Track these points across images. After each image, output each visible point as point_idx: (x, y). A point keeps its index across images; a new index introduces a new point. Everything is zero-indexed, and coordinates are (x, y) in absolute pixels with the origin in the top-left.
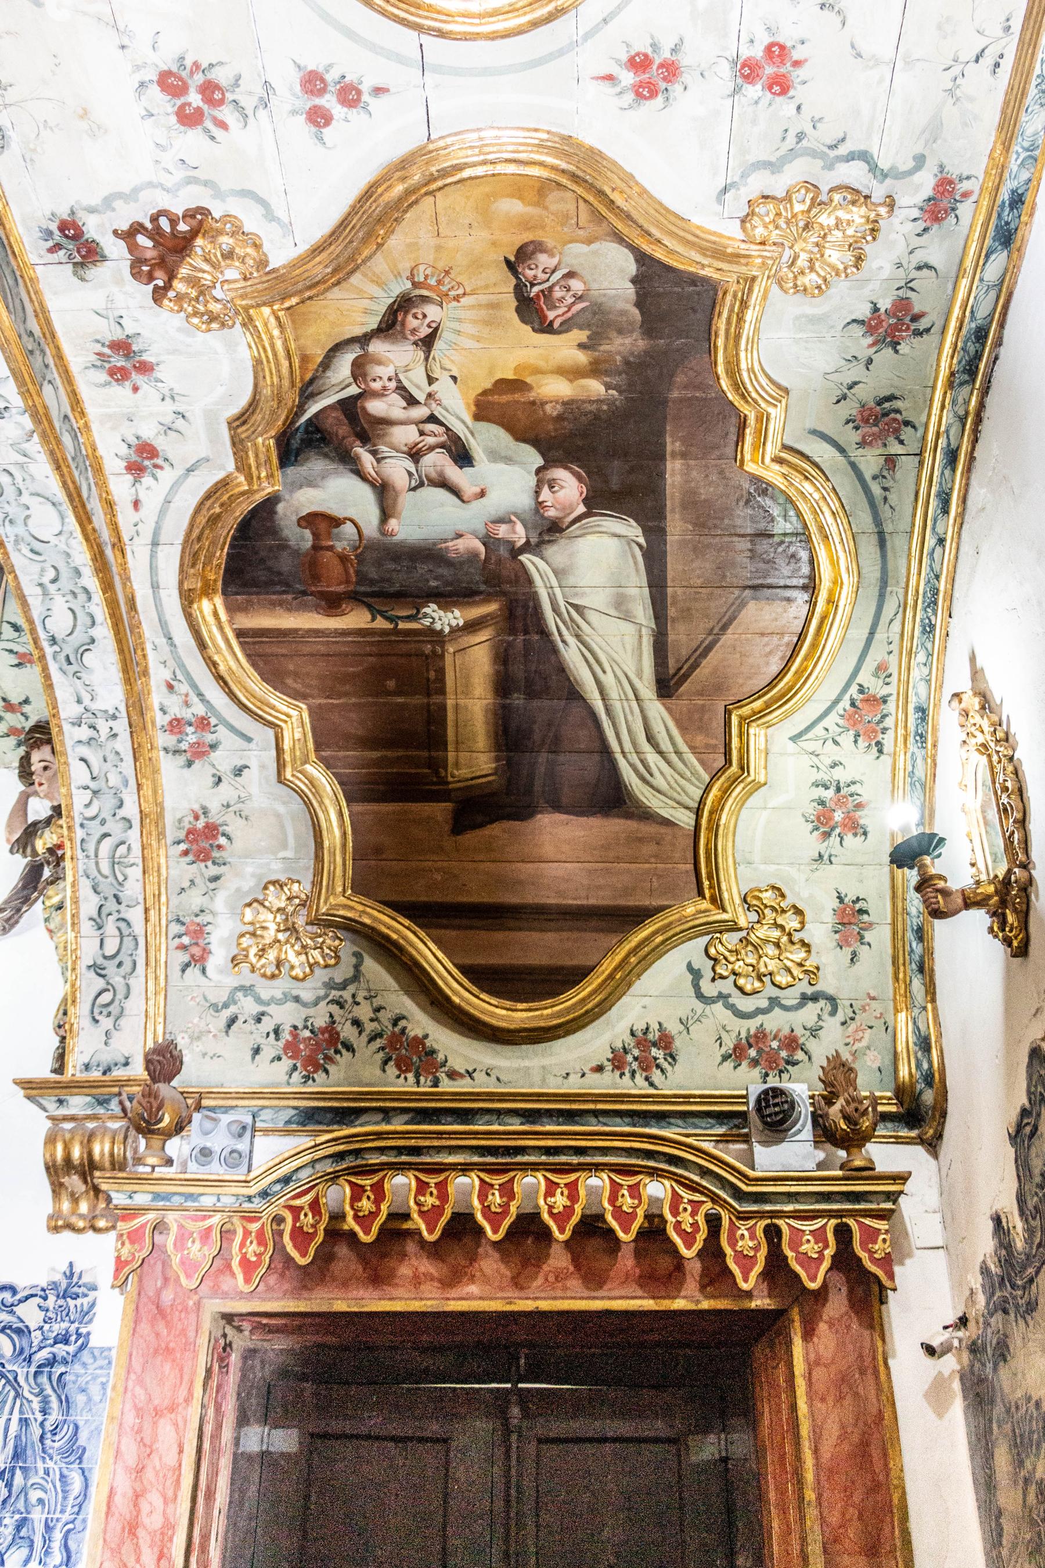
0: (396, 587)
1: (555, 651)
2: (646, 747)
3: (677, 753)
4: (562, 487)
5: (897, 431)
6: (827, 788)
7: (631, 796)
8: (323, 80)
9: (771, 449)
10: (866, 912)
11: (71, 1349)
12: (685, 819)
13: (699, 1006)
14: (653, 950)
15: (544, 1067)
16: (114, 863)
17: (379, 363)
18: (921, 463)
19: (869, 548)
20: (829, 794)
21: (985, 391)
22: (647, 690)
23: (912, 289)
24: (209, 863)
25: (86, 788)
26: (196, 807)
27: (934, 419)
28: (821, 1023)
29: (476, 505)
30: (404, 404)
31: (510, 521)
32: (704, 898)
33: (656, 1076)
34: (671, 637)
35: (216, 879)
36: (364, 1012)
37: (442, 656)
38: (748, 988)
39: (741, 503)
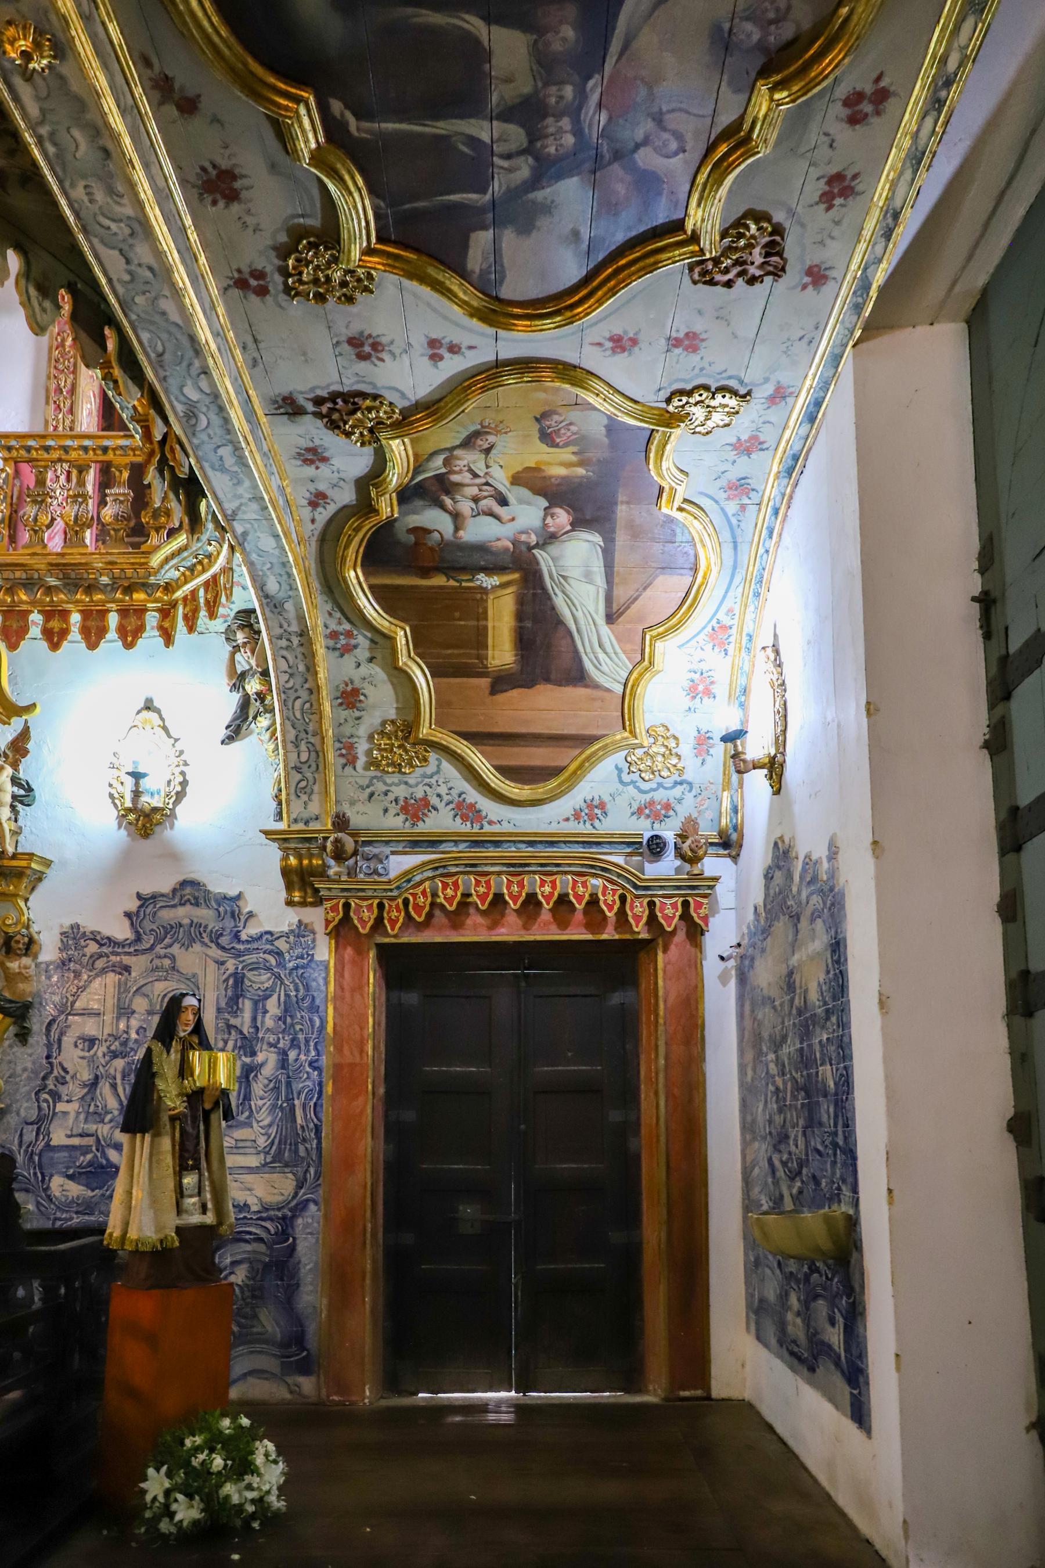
0: (462, 565)
1: (550, 598)
7: (589, 676)
11: (305, 961)
12: (618, 689)
18: (760, 510)
19: (728, 549)
22: (601, 620)
34: (615, 593)
37: (486, 601)
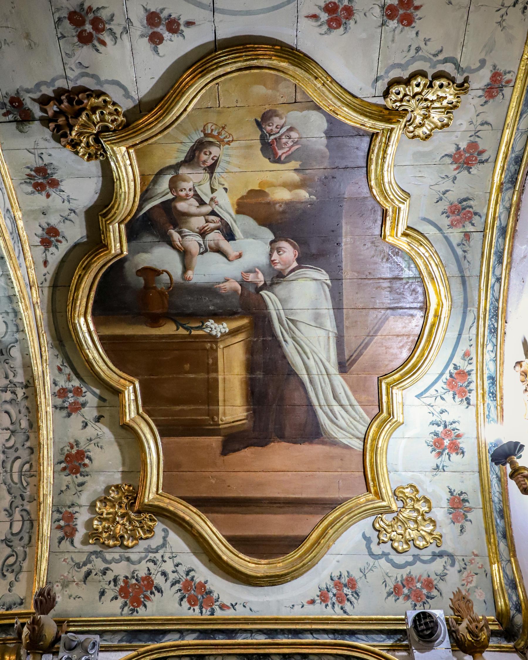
2: (333, 402)
3: (351, 405)
4: (284, 252)
5: (470, 218)
6: (439, 426)
7: (325, 432)
8: (159, 18)
9: (402, 228)
10: (467, 501)
12: (358, 445)
13: (371, 561)
14: (342, 525)
15: (278, 601)
16: (21, 475)
17: (184, 180)
18: (484, 236)
20: (441, 429)
21: (522, 192)
22: (333, 369)
23: (478, 137)
24: (78, 475)
25: (7, 429)
26: (72, 441)
27: (491, 211)
28: (445, 571)
29: (237, 262)
30: (197, 204)
31: (255, 272)
32: (371, 492)
33: (347, 606)
35: (82, 484)
36: (168, 567)
37: (216, 351)
38: (400, 548)
39: (385, 260)
